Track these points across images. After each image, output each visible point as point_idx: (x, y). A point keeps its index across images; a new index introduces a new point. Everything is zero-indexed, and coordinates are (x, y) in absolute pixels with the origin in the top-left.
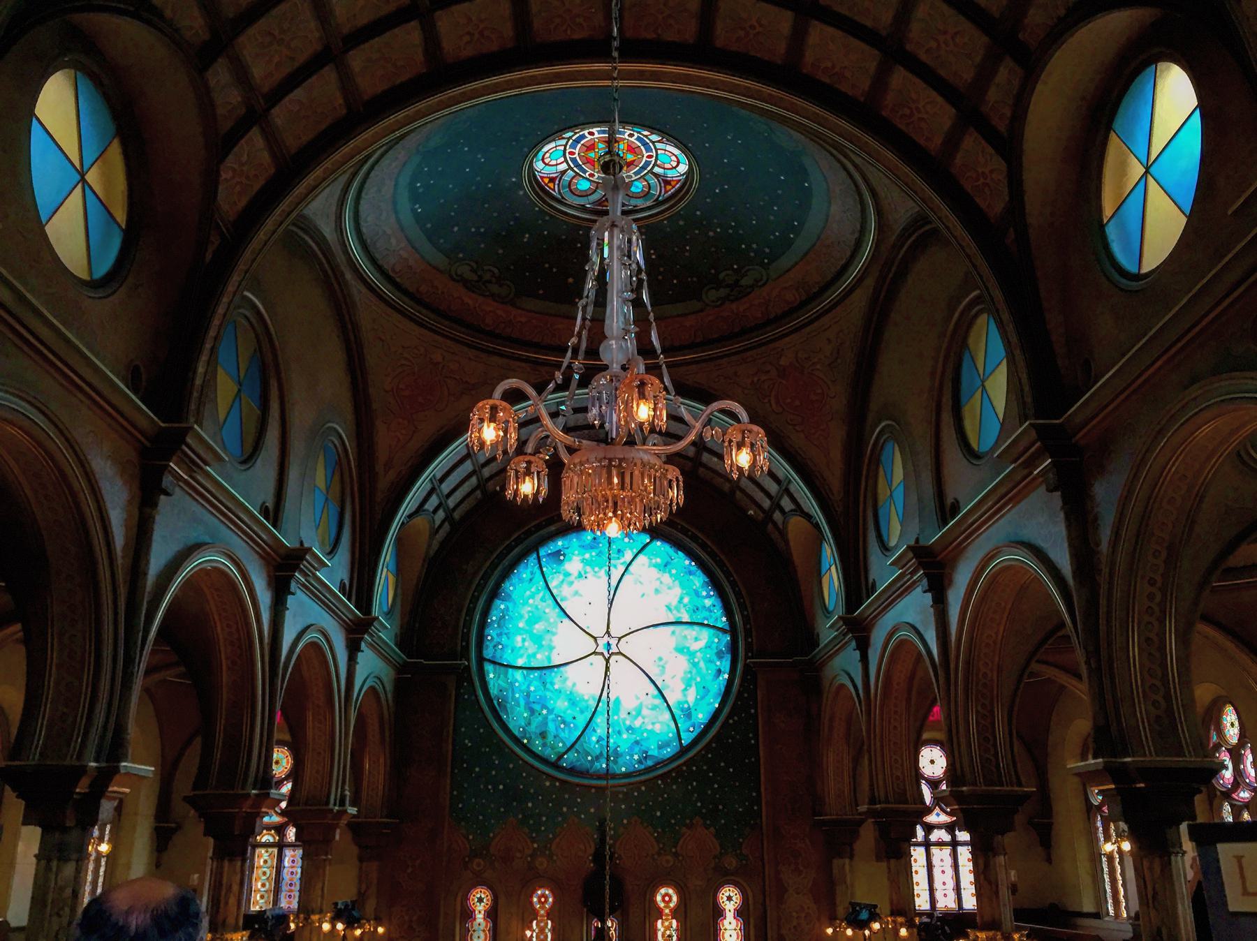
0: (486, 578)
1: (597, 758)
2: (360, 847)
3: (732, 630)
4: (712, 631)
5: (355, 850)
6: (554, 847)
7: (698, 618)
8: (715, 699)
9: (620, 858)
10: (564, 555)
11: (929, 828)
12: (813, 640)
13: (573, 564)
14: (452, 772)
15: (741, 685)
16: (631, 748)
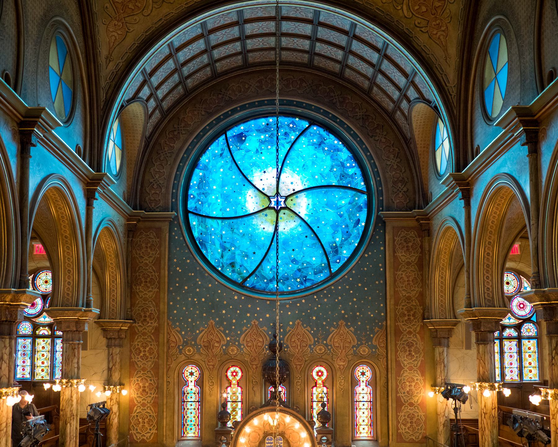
0: (188, 152)
2: (107, 338)
3: (369, 192)
4: (354, 192)
5: (104, 341)
6: (241, 339)
7: (344, 183)
8: (356, 238)
9: (287, 347)
10: (245, 137)
11: (504, 327)
12: (426, 198)
13: (252, 142)
14: (169, 288)
15: (374, 230)
16: (295, 274)
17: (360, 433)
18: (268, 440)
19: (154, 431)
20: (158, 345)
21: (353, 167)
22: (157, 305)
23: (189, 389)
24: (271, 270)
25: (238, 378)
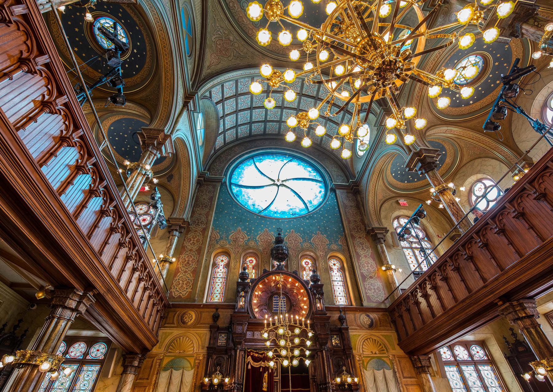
18: (275, 298)
19: (189, 290)
20: (203, 238)
22: (207, 217)
25: (253, 264)
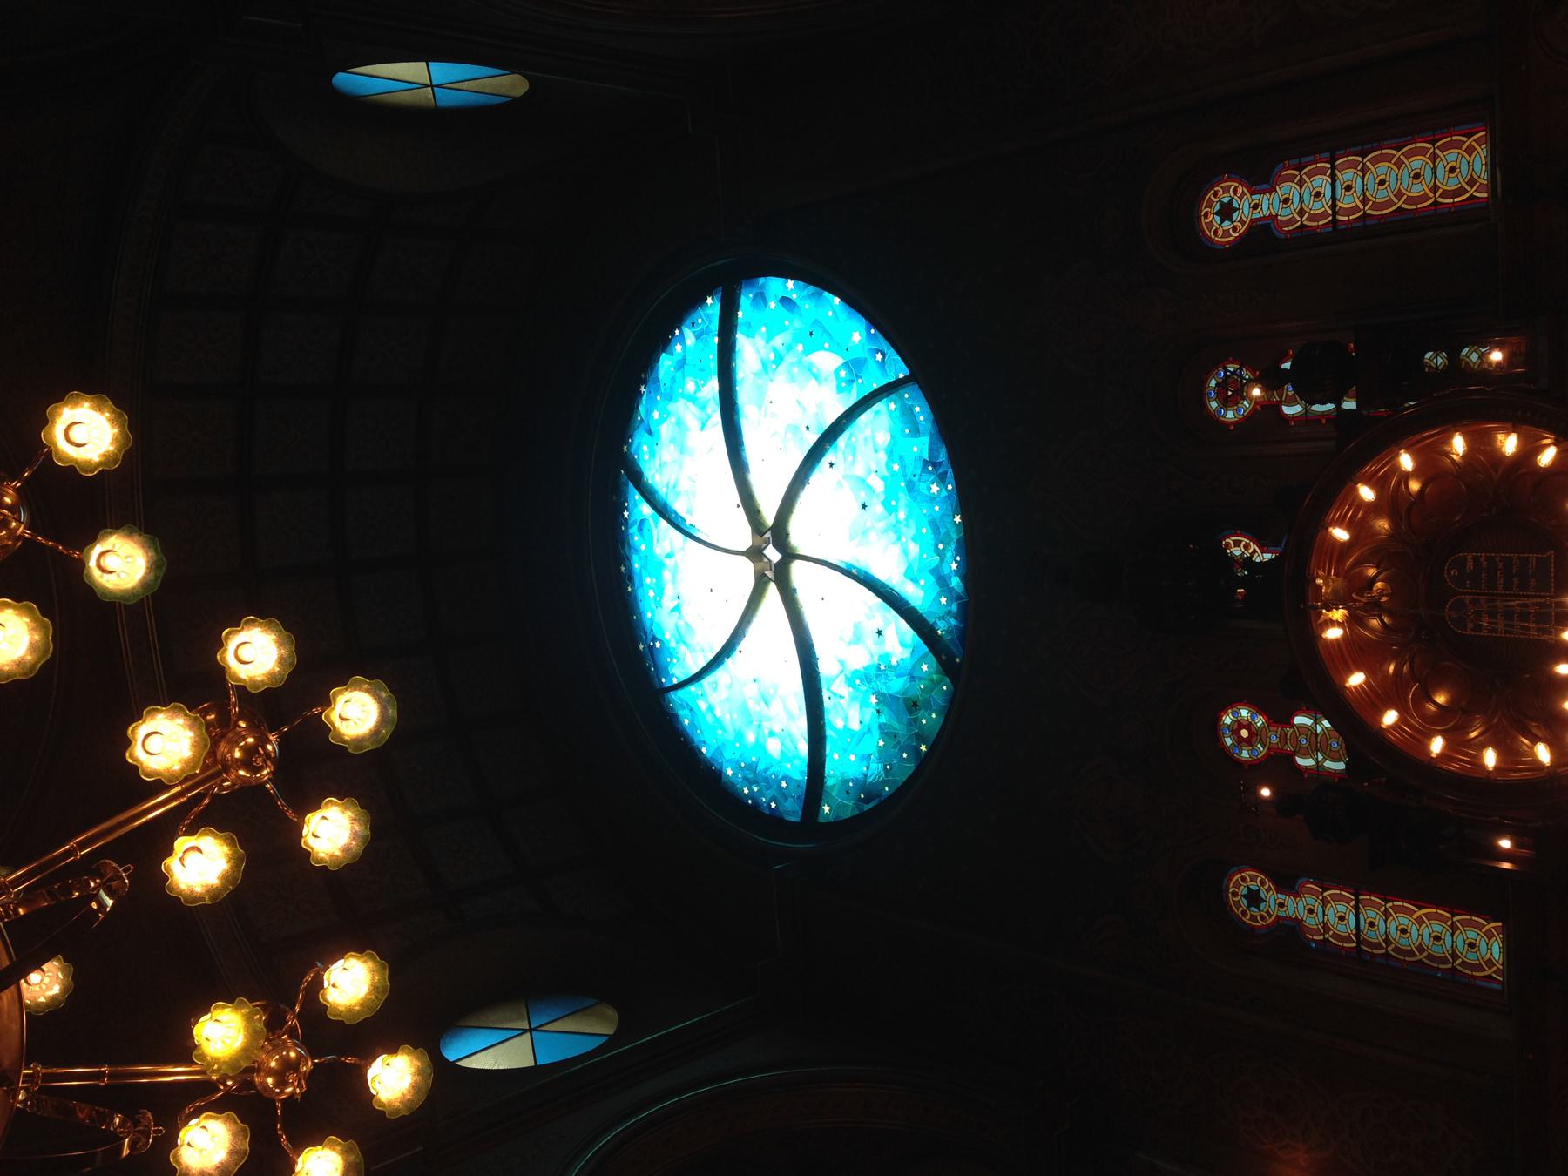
1: (942, 581)
17: (1472, 182)
21: (681, 332)
23: (1311, 922)
24: (915, 581)
